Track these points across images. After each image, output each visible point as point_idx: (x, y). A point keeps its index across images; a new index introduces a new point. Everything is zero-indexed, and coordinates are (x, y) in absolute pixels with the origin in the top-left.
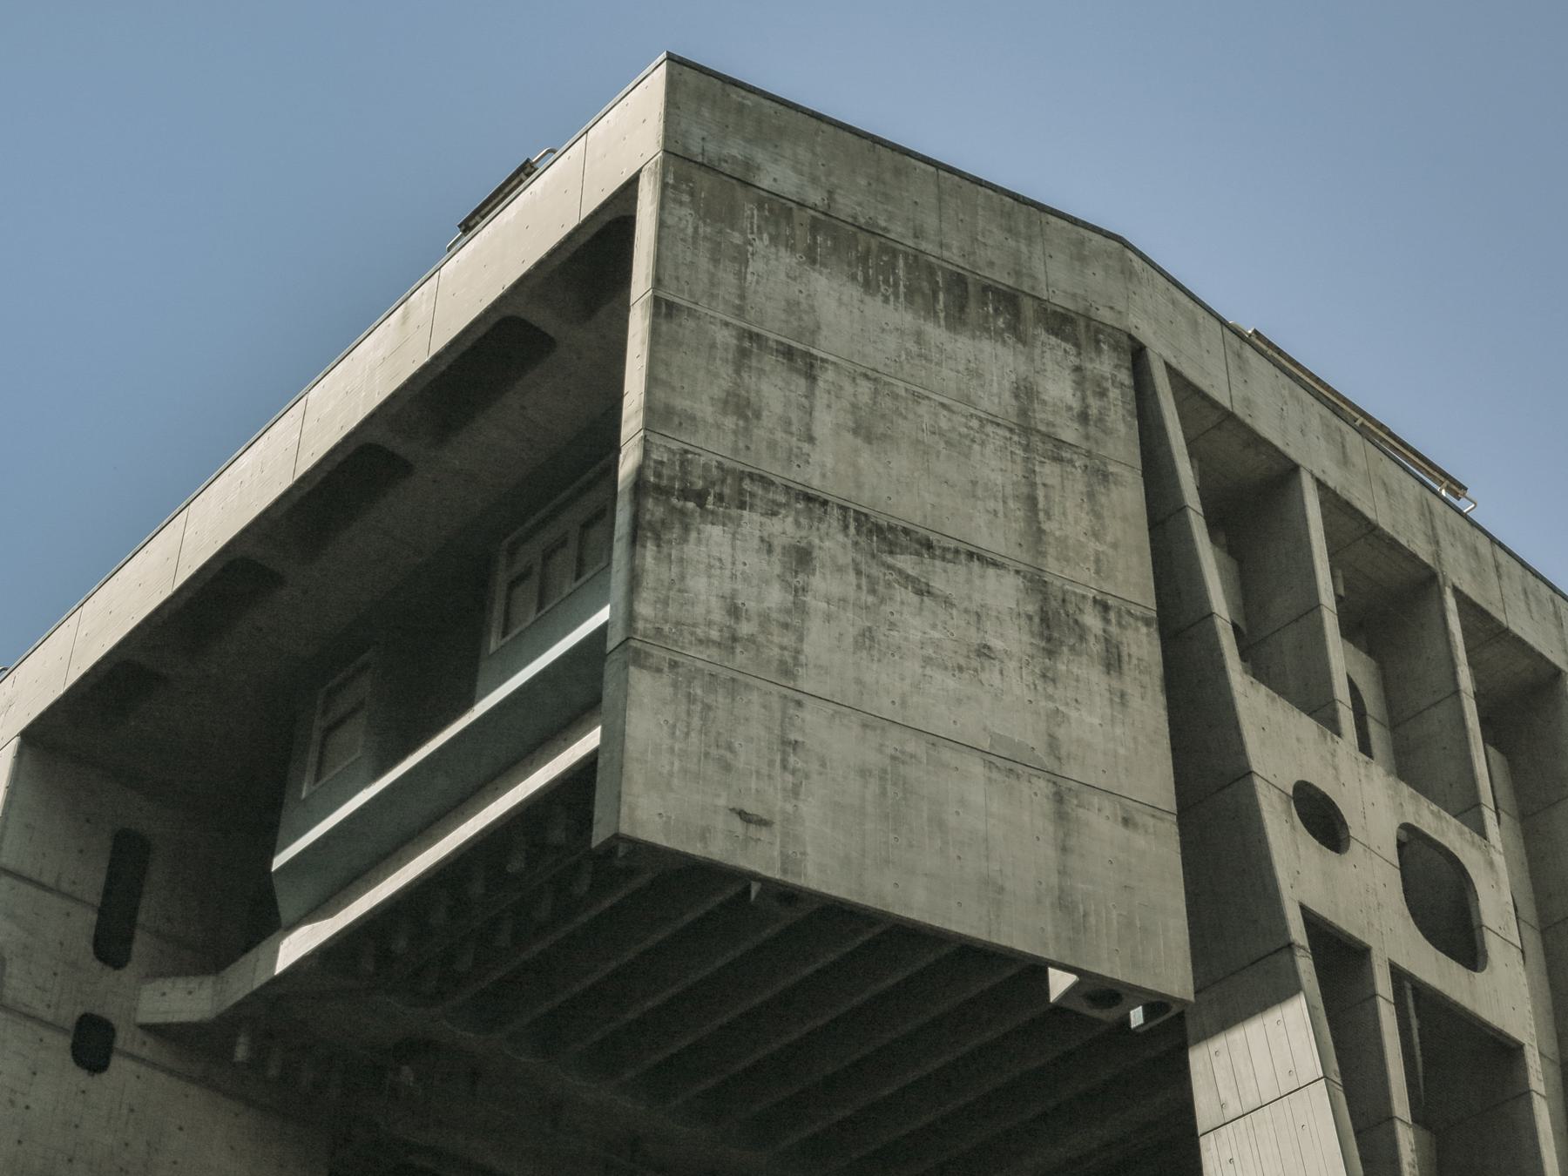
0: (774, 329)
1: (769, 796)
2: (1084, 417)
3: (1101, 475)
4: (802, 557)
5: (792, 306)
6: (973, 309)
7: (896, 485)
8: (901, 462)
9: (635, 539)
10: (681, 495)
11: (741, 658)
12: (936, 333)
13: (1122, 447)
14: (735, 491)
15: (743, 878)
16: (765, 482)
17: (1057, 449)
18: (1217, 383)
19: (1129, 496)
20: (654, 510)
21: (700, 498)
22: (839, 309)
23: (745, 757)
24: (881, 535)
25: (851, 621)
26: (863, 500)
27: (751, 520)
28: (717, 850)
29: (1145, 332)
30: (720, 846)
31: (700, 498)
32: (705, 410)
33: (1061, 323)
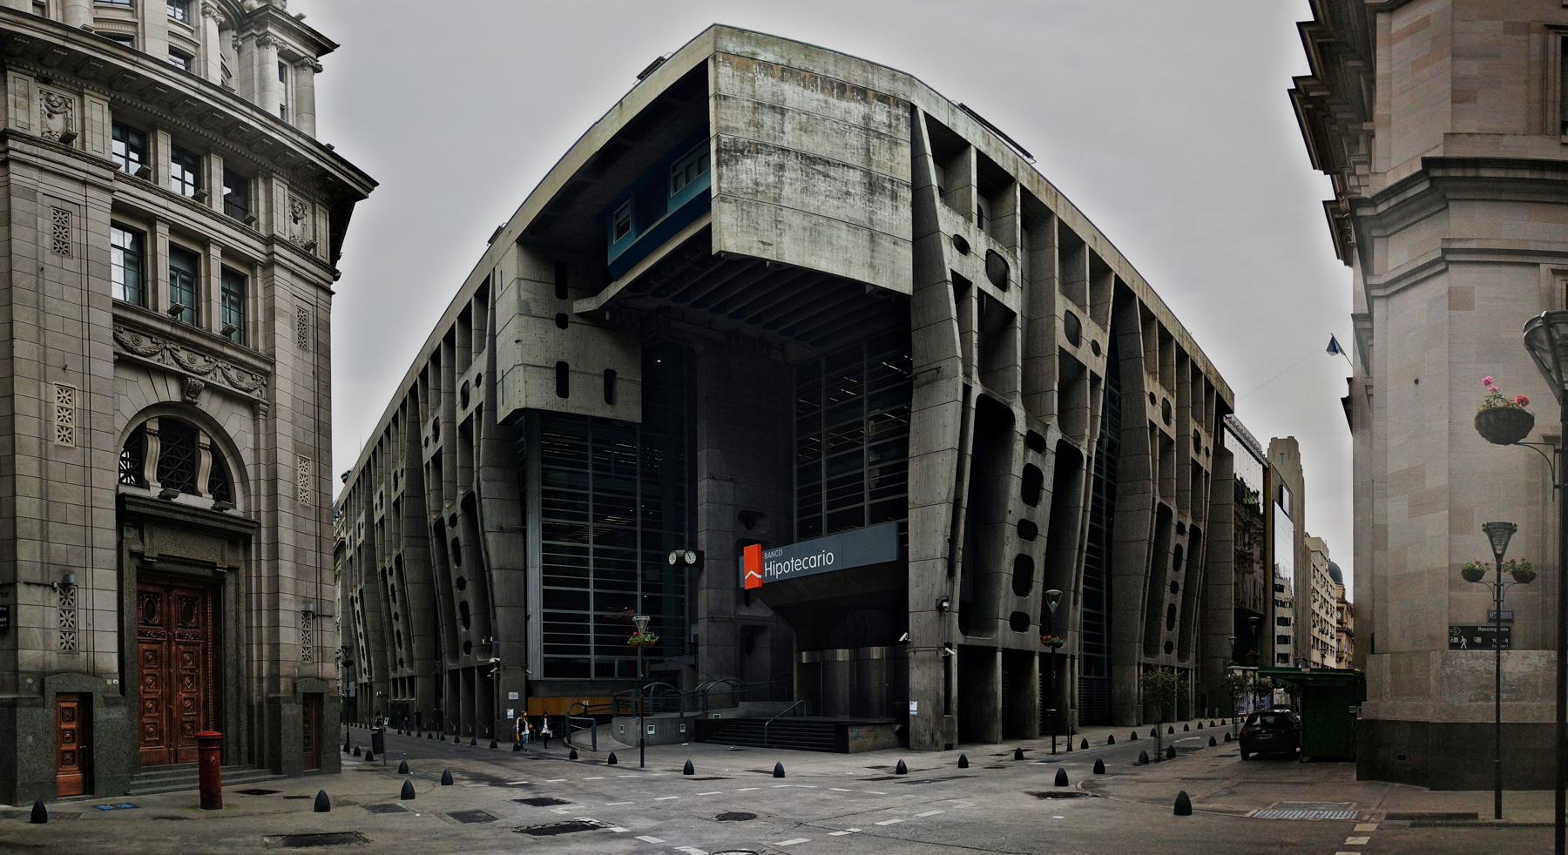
0: (767, 99)
1: (772, 237)
2: (890, 126)
3: (895, 143)
4: (781, 167)
5: (773, 94)
6: (848, 93)
7: (814, 145)
8: (818, 139)
9: (719, 164)
10: (734, 152)
11: (760, 197)
12: (833, 101)
13: (904, 134)
14: (755, 149)
15: (764, 261)
16: (766, 146)
17: (879, 135)
18: (943, 117)
19: (906, 151)
20: (725, 156)
21: (742, 152)
22: (792, 93)
23: (763, 225)
24: (809, 160)
25: (799, 186)
26: (804, 149)
27: (761, 158)
28: (754, 253)
29: (917, 102)
30: (756, 251)
31: (742, 152)
32: (741, 125)
33: (883, 98)
